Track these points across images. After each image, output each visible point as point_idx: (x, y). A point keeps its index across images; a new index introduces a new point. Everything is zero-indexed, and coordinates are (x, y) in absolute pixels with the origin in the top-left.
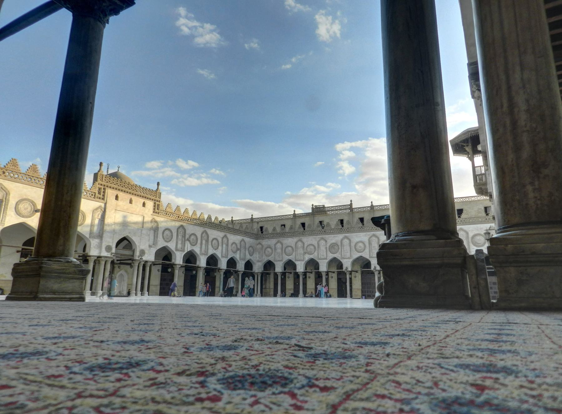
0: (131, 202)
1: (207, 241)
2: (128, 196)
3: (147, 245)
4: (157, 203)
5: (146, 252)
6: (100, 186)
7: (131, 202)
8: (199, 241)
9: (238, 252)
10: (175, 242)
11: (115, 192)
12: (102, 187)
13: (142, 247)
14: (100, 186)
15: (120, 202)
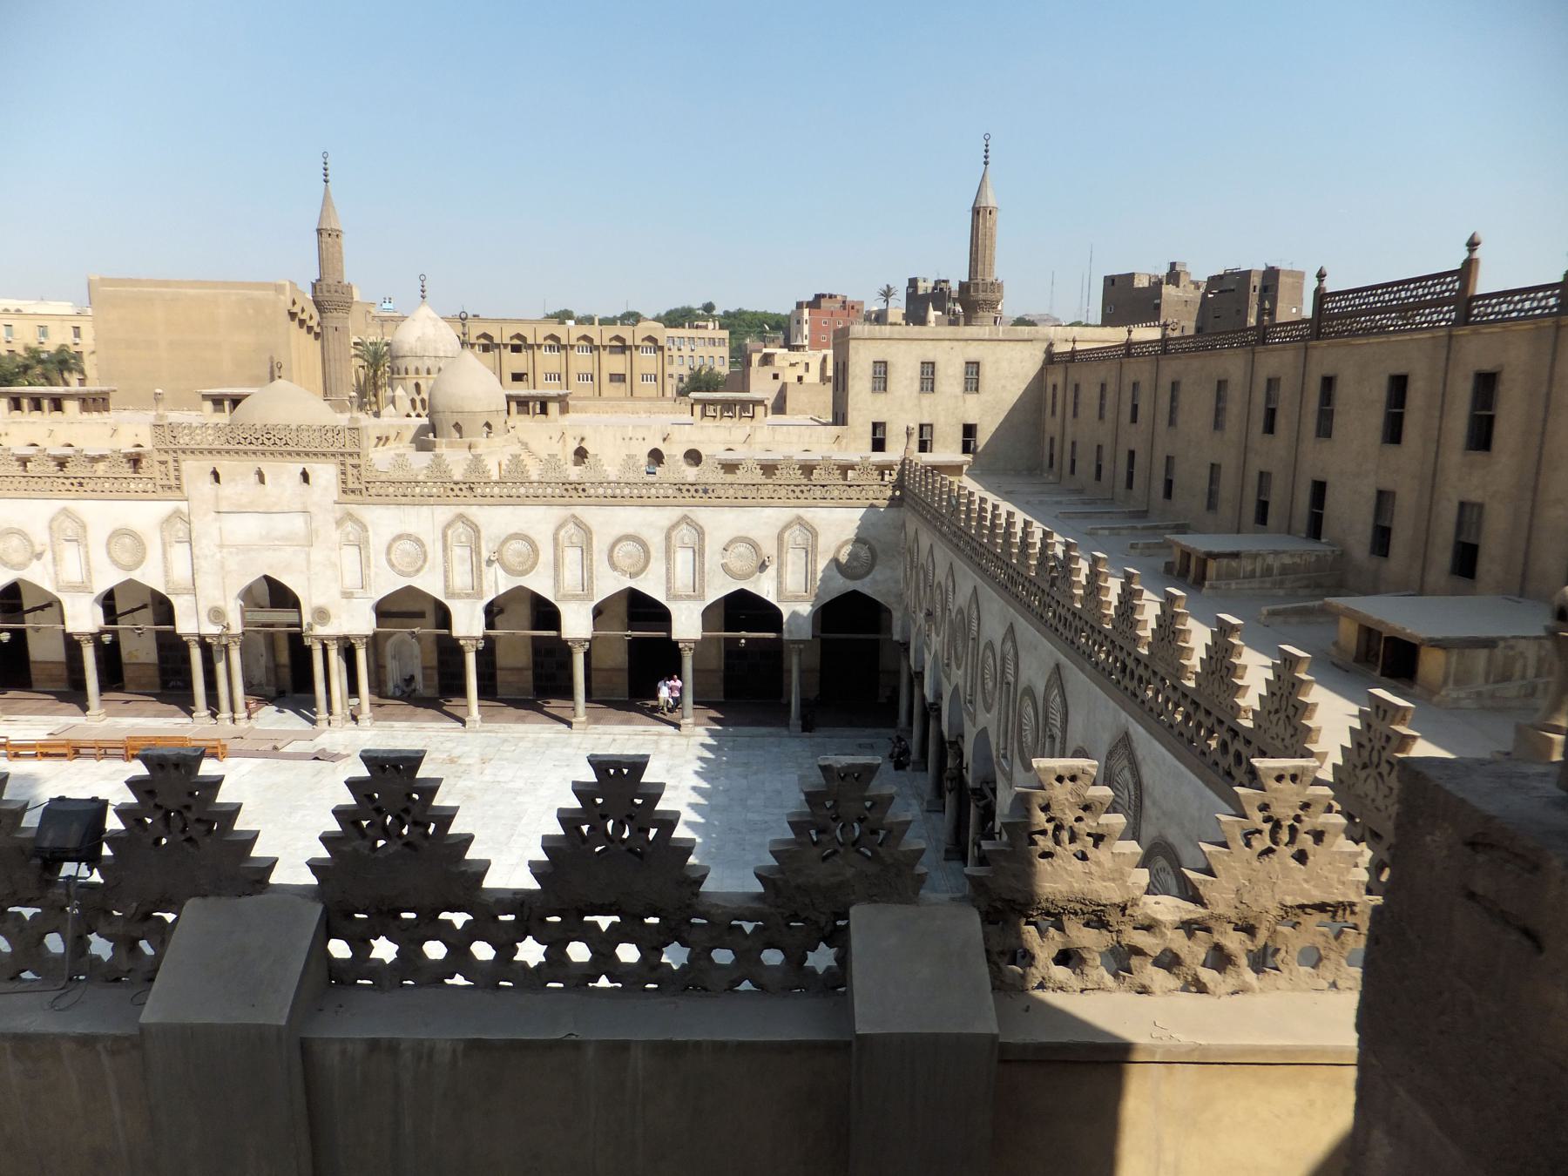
0: (262, 480)
1: (586, 549)
2: (250, 465)
3: (335, 591)
4: (349, 461)
5: (332, 611)
6: (164, 457)
7: (262, 480)
8: (546, 555)
9: (771, 571)
10: (440, 570)
11: (208, 463)
12: (169, 458)
13: (318, 601)
14: (164, 457)
15: (226, 488)
